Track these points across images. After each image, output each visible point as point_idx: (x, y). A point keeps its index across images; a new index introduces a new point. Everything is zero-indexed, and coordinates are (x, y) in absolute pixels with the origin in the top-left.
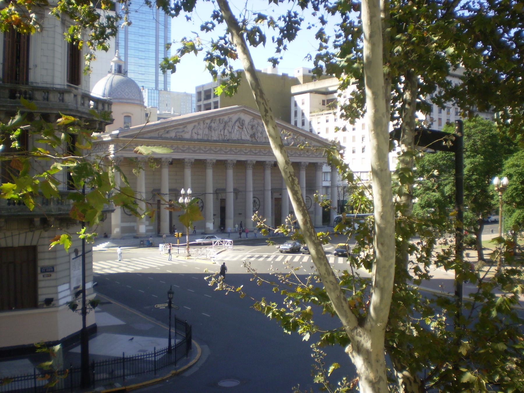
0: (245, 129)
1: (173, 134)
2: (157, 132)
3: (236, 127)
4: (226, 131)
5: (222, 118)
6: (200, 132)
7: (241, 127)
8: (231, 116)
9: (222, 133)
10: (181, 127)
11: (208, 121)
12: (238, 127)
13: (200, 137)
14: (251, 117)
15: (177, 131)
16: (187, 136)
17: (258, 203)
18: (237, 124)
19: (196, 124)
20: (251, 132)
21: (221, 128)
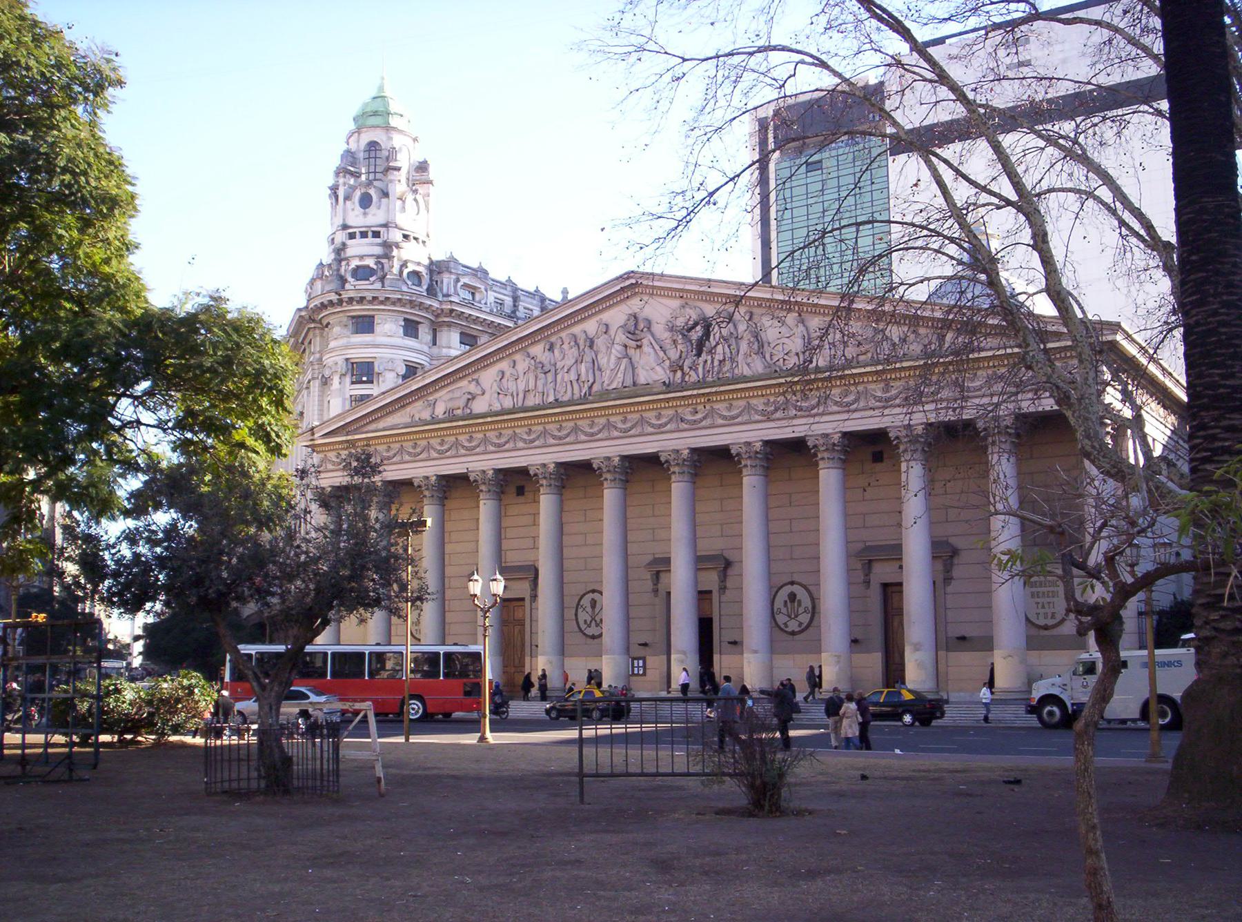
0: (646, 349)
1: (440, 410)
2: (408, 409)
3: (617, 350)
4: (583, 368)
5: (576, 330)
6: (511, 386)
7: (633, 344)
8: (606, 317)
9: (573, 376)
10: (464, 383)
11: (538, 350)
12: (626, 346)
13: (508, 403)
14: (676, 303)
15: (451, 395)
16: (479, 406)
17: (807, 602)
18: (617, 340)
19: (504, 365)
20: (674, 354)
21: (569, 361)
